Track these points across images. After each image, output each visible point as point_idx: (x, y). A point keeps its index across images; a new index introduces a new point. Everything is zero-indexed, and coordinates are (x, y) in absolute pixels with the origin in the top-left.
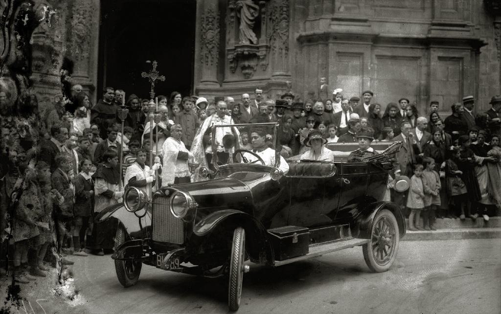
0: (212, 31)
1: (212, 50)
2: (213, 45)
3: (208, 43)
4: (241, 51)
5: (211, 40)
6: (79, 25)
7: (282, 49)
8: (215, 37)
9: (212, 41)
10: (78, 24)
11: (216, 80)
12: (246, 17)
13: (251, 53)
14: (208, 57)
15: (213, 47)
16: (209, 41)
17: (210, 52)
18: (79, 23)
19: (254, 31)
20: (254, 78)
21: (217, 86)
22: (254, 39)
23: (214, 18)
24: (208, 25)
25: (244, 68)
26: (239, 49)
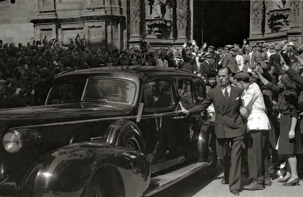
1: (258, 14)
2: (258, 11)
3: (255, 11)
4: (272, 14)
5: (257, 8)
6: (179, 10)
7: (295, 10)
8: (259, 6)
9: (257, 9)
10: (179, 9)
11: (262, 33)
13: (279, 14)
14: (255, 20)
15: (259, 13)
16: (255, 9)
17: (256, 16)
18: (180, 8)
20: (282, 30)
21: (261, 37)
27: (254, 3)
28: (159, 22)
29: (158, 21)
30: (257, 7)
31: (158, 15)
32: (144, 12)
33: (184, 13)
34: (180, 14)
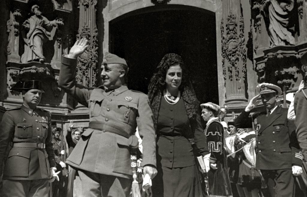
0: (234, 40)
1: (237, 62)
2: (236, 56)
3: (230, 55)
5: (234, 50)
8: (239, 47)
9: (235, 52)
12: (277, 13)
13: (288, 56)
14: (231, 72)
15: (237, 59)
16: (231, 52)
17: (233, 65)
19: (288, 28)
22: (292, 40)
23: (236, 25)
24: (228, 34)
25: (281, 77)
26: (270, 54)
27: (228, 41)
28: (35, 69)
29: (34, 67)
30: (235, 49)
31: (36, 55)
32: (6, 48)
33: (91, 57)
34: (82, 60)
